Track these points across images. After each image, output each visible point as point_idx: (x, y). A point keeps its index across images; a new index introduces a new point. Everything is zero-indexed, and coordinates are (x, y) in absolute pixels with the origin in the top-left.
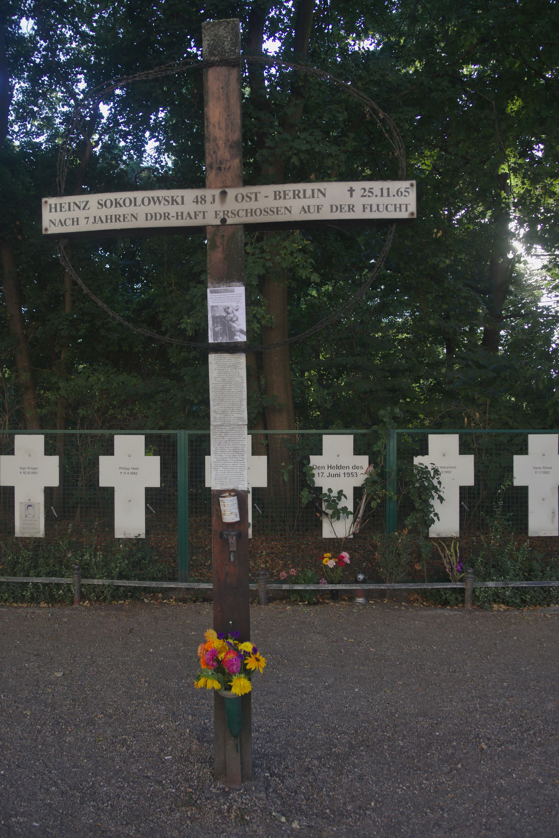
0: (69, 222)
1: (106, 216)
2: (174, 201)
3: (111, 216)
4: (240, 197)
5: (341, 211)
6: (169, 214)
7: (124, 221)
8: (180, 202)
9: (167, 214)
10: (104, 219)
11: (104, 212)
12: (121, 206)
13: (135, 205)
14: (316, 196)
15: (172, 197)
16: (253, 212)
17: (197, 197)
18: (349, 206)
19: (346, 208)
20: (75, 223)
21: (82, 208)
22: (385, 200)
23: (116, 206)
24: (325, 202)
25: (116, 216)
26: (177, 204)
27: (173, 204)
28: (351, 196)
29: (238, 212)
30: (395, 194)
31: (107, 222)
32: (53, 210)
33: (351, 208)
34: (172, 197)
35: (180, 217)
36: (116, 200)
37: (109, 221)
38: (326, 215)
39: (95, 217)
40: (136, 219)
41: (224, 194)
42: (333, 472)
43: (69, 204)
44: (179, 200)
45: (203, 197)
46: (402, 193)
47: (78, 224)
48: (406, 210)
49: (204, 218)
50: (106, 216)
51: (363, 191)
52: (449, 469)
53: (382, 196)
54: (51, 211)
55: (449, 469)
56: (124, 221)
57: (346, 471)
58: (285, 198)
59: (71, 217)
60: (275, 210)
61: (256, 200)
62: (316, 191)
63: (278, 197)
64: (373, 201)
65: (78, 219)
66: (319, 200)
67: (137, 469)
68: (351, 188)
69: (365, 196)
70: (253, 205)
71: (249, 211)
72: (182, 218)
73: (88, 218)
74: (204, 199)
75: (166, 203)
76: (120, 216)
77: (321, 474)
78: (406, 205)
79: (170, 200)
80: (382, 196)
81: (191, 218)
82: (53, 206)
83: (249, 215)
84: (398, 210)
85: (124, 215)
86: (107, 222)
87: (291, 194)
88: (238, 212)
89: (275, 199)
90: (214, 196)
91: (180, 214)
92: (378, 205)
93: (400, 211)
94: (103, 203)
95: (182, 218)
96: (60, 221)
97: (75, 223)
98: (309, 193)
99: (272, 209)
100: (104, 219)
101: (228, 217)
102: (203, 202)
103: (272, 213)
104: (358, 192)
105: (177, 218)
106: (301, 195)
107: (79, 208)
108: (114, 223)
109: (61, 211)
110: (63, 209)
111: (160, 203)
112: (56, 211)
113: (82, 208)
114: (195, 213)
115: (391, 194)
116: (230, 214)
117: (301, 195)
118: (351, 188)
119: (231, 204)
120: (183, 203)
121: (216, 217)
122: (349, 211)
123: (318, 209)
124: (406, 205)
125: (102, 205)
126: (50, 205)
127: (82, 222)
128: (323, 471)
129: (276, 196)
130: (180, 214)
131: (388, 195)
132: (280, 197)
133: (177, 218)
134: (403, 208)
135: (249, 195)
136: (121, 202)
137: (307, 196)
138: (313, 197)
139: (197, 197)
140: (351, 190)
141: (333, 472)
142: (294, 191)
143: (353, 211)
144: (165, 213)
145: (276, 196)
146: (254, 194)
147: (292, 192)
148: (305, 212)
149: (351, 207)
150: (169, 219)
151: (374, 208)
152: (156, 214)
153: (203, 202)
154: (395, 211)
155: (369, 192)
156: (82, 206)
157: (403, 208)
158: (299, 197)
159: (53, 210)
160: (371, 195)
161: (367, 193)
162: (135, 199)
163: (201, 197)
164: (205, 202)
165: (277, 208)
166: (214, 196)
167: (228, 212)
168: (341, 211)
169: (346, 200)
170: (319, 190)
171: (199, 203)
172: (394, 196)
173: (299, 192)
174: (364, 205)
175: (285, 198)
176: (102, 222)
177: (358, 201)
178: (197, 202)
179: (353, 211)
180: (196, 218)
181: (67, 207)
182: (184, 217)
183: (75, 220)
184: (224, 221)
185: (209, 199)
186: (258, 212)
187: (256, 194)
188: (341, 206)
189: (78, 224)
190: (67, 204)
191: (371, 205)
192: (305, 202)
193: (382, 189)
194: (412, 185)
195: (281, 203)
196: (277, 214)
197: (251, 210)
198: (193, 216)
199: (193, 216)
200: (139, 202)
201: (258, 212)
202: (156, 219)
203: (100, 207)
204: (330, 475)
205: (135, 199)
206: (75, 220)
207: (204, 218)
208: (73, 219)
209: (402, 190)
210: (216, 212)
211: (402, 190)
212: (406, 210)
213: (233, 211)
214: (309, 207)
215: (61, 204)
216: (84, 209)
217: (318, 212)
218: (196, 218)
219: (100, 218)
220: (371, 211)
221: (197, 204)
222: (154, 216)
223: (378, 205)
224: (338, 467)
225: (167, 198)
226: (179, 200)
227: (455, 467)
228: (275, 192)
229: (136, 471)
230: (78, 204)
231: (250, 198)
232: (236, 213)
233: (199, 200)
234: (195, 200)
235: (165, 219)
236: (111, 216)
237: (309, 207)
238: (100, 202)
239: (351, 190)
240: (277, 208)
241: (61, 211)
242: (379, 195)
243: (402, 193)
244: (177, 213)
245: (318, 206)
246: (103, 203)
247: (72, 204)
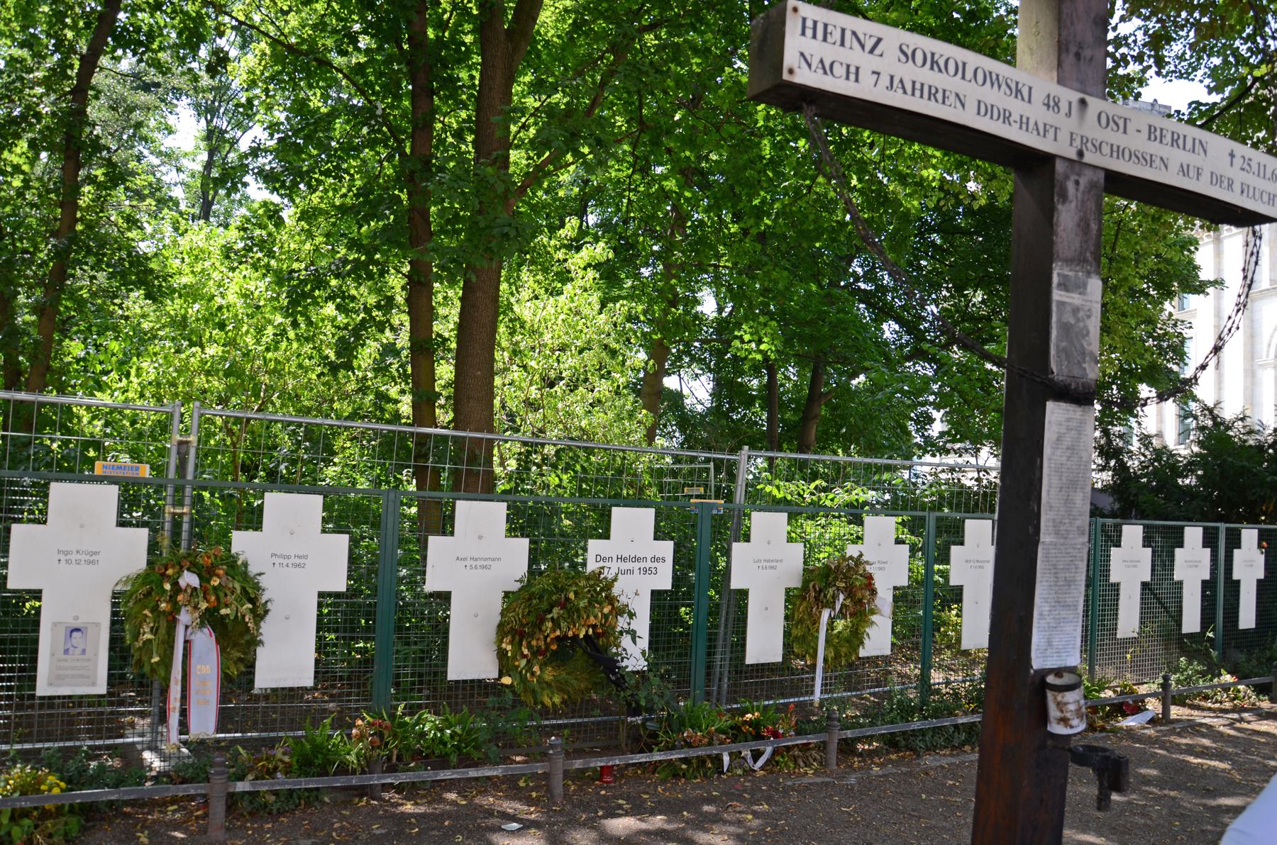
0: (839, 70)
1: (914, 83)
11: (909, 72)
12: (940, 71)
13: (963, 77)
17: (1049, 96)
20: (852, 77)
21: (868, 48)
23: (932, 68)
31: (913, 94)
32: (809, 32)
36: (933, 55)
37: (918, 93)
39: (892, 77)
40: (963, 105)
43: (843, 31)
47: (857, 80)
50: (914, 83)
54: (803, 34)
59: (846, 61)
65: (857, 69)
76: (937, 91)
82: (809, 24)
85: (944, 91)
94: (909, 53)
96: (821, 61)
97: (852, 77)
107: (863, 46)
108: (925, 101)
109: (825, 39)
111: (1000, 87)
116: (1089, 145)
125: (908, 55)
126: (804, 20)
159: (809, 32)
178: (1048, 106)
183: (853, 70)
189: (857, 80)
203: (903, 59)
205: (964, 64)
206: (853, 70)
215: (826, 26)
216: (871, 51)
219: (901, 81)
233: (1052, 103)
238: (904, 48)
241: (825, 39)
246: (909, 53)
247: (848, 35)
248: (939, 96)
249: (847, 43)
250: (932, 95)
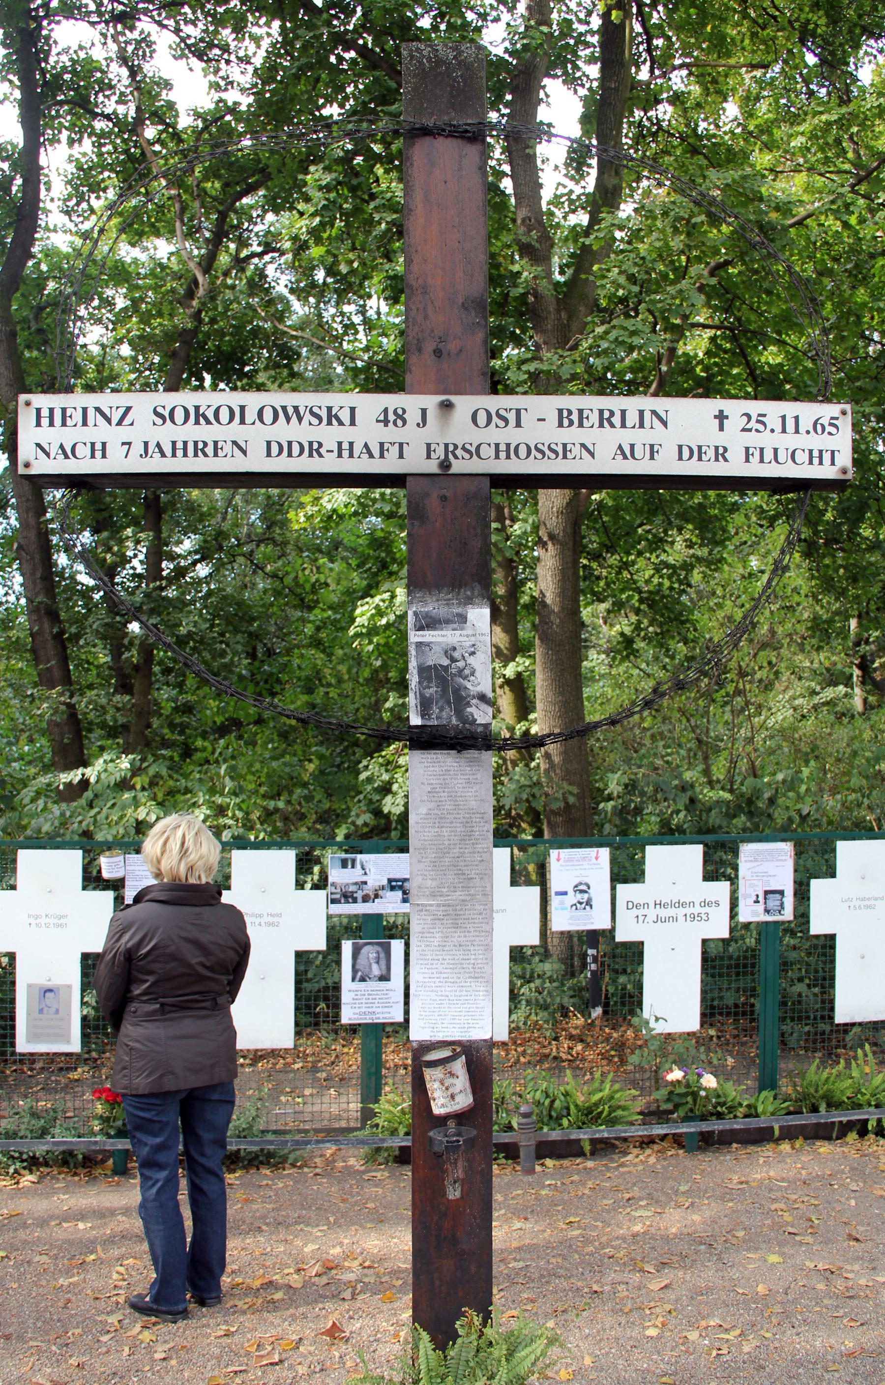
0: (83, 451)
1: (174, 443)
2: (332, 417)
3: (185, 443)
4: (482, 418)
5: (700, 459)
6: (320, 445)
7: (216, 455)
8: (346, 419)
9: (315, 446)
13: (243, 422)
14: (647, 423)
15: (329, 409)
16: (511, 451)
17: (386, 411)
18: (717, 448)
19: (711, 453)
21: (115, 421)
22: (790, 441)
23: (197, 422)
24: (668, 440)
25: (196, 443)
26: (341, 423)
27: (330, 423)
28: (721, 428)
29: (478, 448)
30: (811, 429)
31: (174, 455)
32: (45, 422)
33: (721, 454)
34: (329, 409)
35: (346, 454)
36: (197, 408)
37: (180, 453)
38: (667, 464)
39: (146, 444)
41: (447, 406)
42: (664, 913)
43: (85, 410)
44: (345, 416)
45: (400, 412)
46: (823, 426)
48: (833, 464)
49: (401, 456)
50: (174, 443)
51: (745, 419)
52: (872, 902)
53: (784, 431)
54: (38, 424)
55: (872, 902)
56: (216, 455)
57: (688, 911)
58: (581, 425)
60: (560, 449)
61: (518, 425)
62: (647, 415)
63: (566, 422)
64: (767, 440)
65: (104, 445)
66: (654, 434)
68: (721, 412)
69: (750, 430)
70: (510, 435)
71: (503, 447)
72: (351, 456)
73: (129, 444)
74: (401, 417)
75: (315, 421)
76: (205, 444)
77: (641, 919)
78: (833, 452)
79: (324, 414)
80: (784, 431)
81: (371, 456)
82: (45, 413)
83: (503, 455)
84: (816, 461)
85: (216, 443)
86: (174, 455)
87: (594, 418)
88: (478, 448)
89: (561, 425)
90: (424, 412)
91: (345, 446)
92: (776, 450)
93: (821, 463)
95: (351, 456)
96: (62, 447)
97: (98, 454)
98: (632, 418)
99: (553, 446)
101: (456, 457)
102: (400, 423)
103: (553, 456)
104: (735, 423)
105: (340, 455)
106: (616, 420)
107: (109, 420)
110: (69, 422)
111: (300, 419)
112: (52, 424)
113: (115, 421)
114: (382, 445)
115: (802, 429)
116: (459, 452)
117: (616, 420)
118: (721, 412)
119: (461, 429)
120: (353, 423)
121: (429, 457)
122: (717, 460)
123: (652, 453)
124: (833, 452)
126: (38, 411)
128: (645, 911)
129: (563, 418)
130: (345, 446)
131: (797, 431)
132: (571, 423)
133: (340, 455)
134: (827, 457)
135: (502, 412)
136: (210, 414)
137: (629, 424)
138: (642, 426)
139: (386, 411)
140: (721, 417)
141: (664, 913)
142: (601, 412)
143: (726, 460)
144: (311, 444)
145: (563, 418)
146: (514, 412)
147: (596, 413)
148: (625, 457)
149: (721, 451)
150: (321, 456)
151: (769, 455)
152: (290, 444)
153: (400, 423)
154: (811, 463)
155: (758, 421)
156: (116, 417)
157: (827, 457)
158: (612, 426)
159: (45, 422)
160: (760, 427)
161: (753, 424)
162: (242, 408)
163: (395, 412)
164: (405, 422)
165: (565, 446)
166: (424, 412)
167: (456, 447)
168: (700, 459)
169: (711, 437)
170: (654, 412)
171: (391, 424)
172: (808, 432)
173: (612, 413)
174: (747, 449)
175: (581, 425)
176: (163, 455)
177: (734, 439)
178: (386, 422)
179: (726, 460)
180: (382, 456)
181: (78, 416)
182: (356, 453)
183: (98, 446)
184: (445, 465)
185: (413, 417)
187: (518, 412)
188: (700, 447)
190: (80, 411)
191: (762, 450)
192: (625, 437)
193: (784, 418)
194: (844, 413)
195: (572, 435)
196: (565, 457)
197: (508, 445)
198: (376, 452)
199: (376, 452)
202: (290, 455)
203: (159, 421)
204: (658, 920)
205: (242, 408)
206: (98, 446)
207: (401, 456)
208: (93, 445)
209: (825, 421)
210: (428, 446)
211: (825, 421)
212: (833, 464)
213: (468, 446)
214: (632, 446)
215: (64, 410)
216: (119, 423)
217: (652, 458)
218: (382, 456)
219: (158, 445)
220: (762, 461)
221: (386, 425)
223: (776, 450)
224: (672, 905)
225: (315, 410)
226: (345, 416)
227: (882, 899)
228: (560, 411)
230: (107, 412)
231: (506, 421)
232: (473, 450)
234: (382, 418)
235: (311, 455)
236: (185, 443)
237: (632, 446)
238: (160, 410)
239: (721, 417)
240: (565, 446)
241: (64, 424)
242: (779, 429)
243: (823, 426)
244: (340, 444)
245: (652, 446)
247: (91, 413)
248: (210, 450)
249: (90, 421)
250: (199, 449)
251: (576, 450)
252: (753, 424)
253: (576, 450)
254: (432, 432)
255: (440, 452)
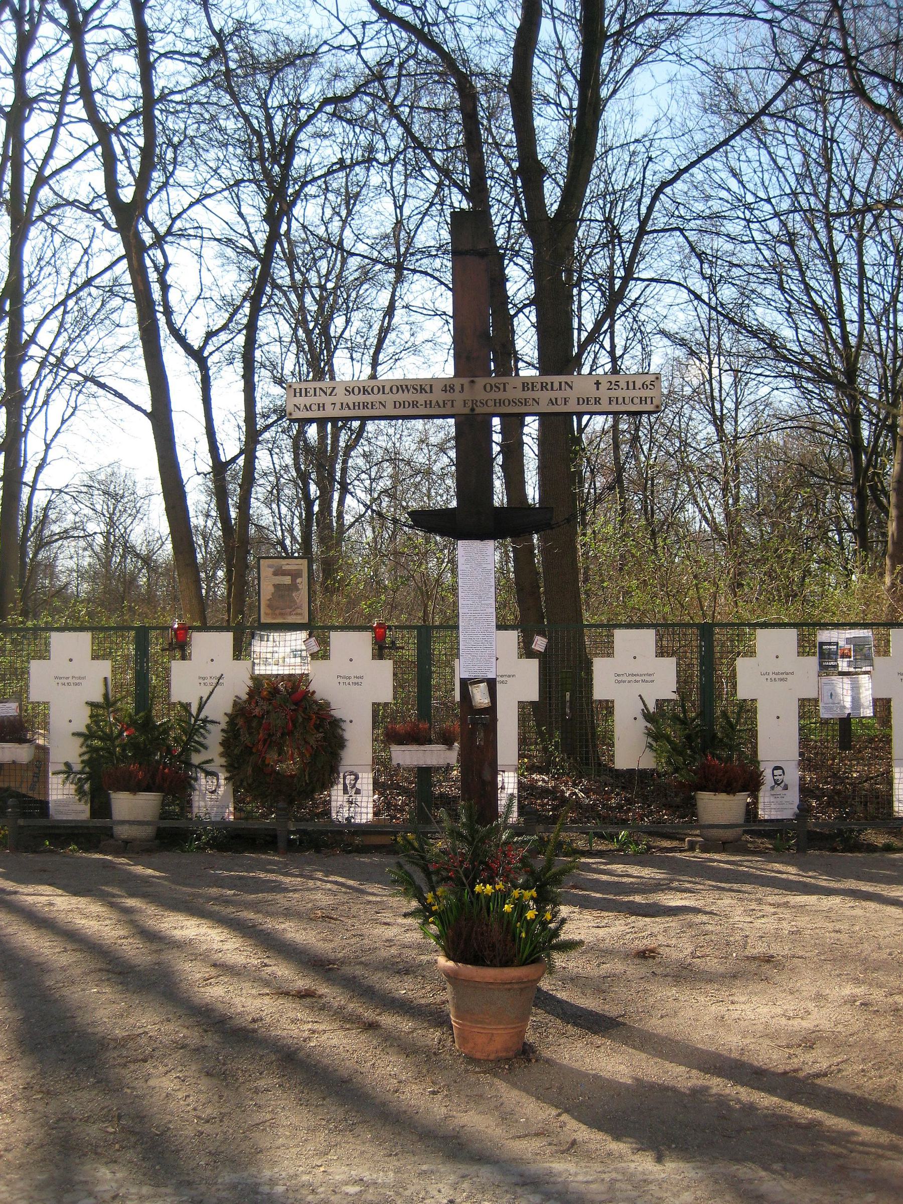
0: (314, 407)
4: (488, 388)
10: (351, 406)
11: (351, 399)
19: (593, 401)
22: (631, 393)
33: (597, 401)
44: (428, 389)
64: (619, 393)
66: (567, 393)
67: (362, 677)
70: (501, 395)
87: (539, 386)
98: (556, 386)
100: (351, 406)
106: (549, 387)
117: (549, 387)
123: (566, 401)
127: (329, 407)
134: (649, 401)
151: (621, 400)
157: (649, 401)
181: (312, 392)
184: (473, 410)
186: (507, 403)
195: (529, 394)
200: (387, 390)
201: (507, 403)
209: (648, 383)
211: (648, 383)
222: (402, 404)
226: (428, 389)
229: (359, 680)
251: (531, 402)
252: (613, 386)
253: (531, 402)
254: (466, 395)
255: (470, 404)
